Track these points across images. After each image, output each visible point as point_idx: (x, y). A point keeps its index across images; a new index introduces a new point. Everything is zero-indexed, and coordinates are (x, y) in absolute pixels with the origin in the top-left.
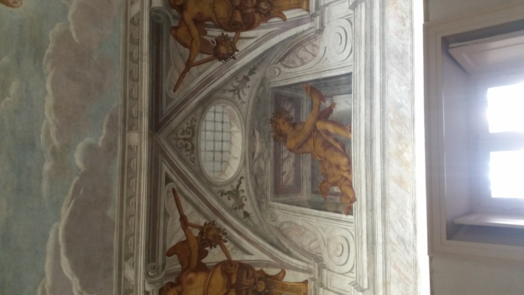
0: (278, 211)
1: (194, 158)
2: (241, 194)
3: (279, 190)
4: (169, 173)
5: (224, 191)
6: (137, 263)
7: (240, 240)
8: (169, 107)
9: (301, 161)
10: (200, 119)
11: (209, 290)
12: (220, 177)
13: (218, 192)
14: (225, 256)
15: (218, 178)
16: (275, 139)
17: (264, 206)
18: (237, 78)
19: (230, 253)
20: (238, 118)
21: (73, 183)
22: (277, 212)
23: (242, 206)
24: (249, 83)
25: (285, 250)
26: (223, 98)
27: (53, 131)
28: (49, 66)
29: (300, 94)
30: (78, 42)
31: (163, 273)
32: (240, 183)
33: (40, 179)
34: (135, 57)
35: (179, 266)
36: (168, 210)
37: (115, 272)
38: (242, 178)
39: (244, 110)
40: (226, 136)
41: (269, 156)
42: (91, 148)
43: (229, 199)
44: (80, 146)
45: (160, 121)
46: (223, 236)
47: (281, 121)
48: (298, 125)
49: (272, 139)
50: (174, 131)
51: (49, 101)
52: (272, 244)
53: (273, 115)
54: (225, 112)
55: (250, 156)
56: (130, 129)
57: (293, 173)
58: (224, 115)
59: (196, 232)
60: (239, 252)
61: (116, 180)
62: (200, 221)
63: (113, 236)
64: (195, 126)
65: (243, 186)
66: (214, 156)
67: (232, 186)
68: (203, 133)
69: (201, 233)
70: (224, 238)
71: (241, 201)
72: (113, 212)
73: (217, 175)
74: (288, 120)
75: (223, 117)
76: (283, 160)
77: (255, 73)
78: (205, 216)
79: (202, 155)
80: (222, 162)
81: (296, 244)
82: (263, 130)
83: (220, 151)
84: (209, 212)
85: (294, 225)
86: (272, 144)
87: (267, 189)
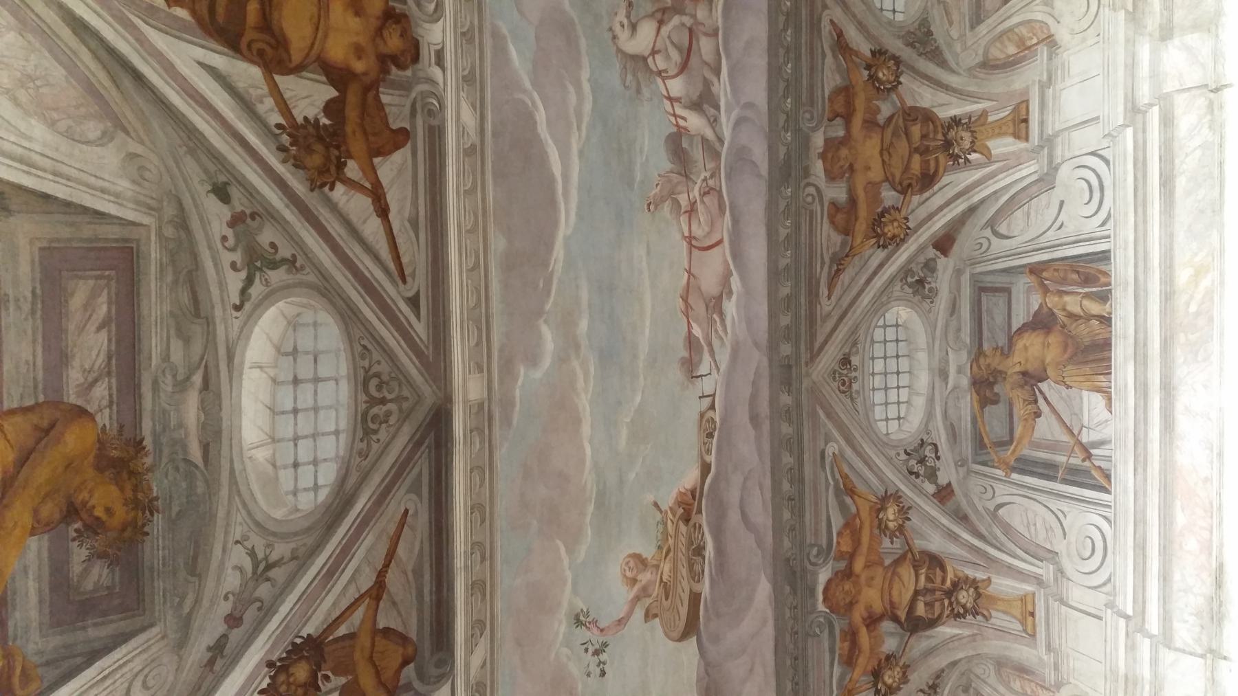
0: (120, 189)
1: (363, 357)
2: (237, 257)
3: (120, 261)
4: (412, 318)
5: (289, 271)
6: (457, 132)
7: (239, 118)
8: (416, 471)
9: (40, 376)
10: (349, 461)
11: (315, 10)
12: (300, 310)
13: (302, 268)
14: (281, 86)
15: (303, 306)
16: (138, 445)
17: (170, 211)
18: (260, 609)
19: (266, 90)
20: (255, 487)
21: (552, 299)
22: (124, 185)
23: (236, 220)
24: (225, 608)
25: (94, 44)
26: (296, 534)
27: (580, 384)
28: (589, 486)
29: (55, 641)
30: (559, 543)
31: (413, 95)
32: (244, 292)
33: (590, 306)
34: (477, 556)
35: (385, 99)
36: (412, 234)
37: (489, 127)
38: (238, 308)
39: (239, 517)
40: (286, 428)
41: (155, 383)
42: (533, 360)
43: (273, 245)
44: (547, 362)
45: (432, 434)
46: (287, 144)
47: (121, 513)
48: (57, 516)
49: (148, 443)
50: (405, 417)
51: (586, 429)
52: (138, 77)
53: (146, 529)
54: (290, 497)
55: (212, 380)
56: (481, 406)
57: (72, 327)
58: (292, 488)
59: (352, 169)
60: (241, 85)
61: (496, 305)
62: (345, 198)
63: (494, 198)
64: (362, 440)
65: (235, 282)
66: (316, 369)
67: (267, 283)
68: (343, 425)
69: (341, 166)
70: (285, 139)
71: (236, 236)
72: (498, 243)
73: (308, 317)
74: (94, 527)
75: (296, 479)
76: (109, 374)
77: (209, 649)
78: (334, 207)
79: (344, 369)
80: (295, 352)
81: (50, 51)
82: (177, 469)
83: (302, 381)
84: (325, 215)
85: (62, 125)
86: (147, 426)
87: (162, 269)
